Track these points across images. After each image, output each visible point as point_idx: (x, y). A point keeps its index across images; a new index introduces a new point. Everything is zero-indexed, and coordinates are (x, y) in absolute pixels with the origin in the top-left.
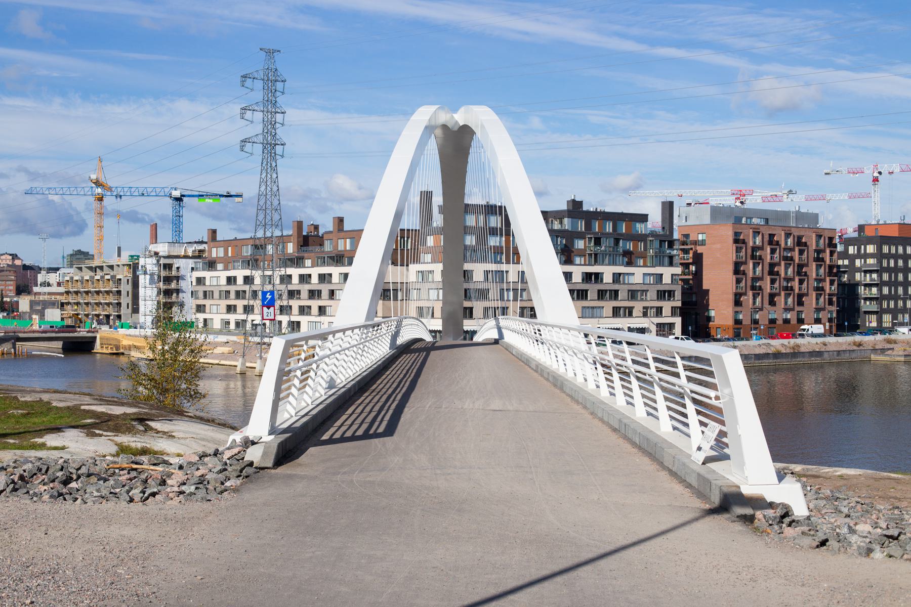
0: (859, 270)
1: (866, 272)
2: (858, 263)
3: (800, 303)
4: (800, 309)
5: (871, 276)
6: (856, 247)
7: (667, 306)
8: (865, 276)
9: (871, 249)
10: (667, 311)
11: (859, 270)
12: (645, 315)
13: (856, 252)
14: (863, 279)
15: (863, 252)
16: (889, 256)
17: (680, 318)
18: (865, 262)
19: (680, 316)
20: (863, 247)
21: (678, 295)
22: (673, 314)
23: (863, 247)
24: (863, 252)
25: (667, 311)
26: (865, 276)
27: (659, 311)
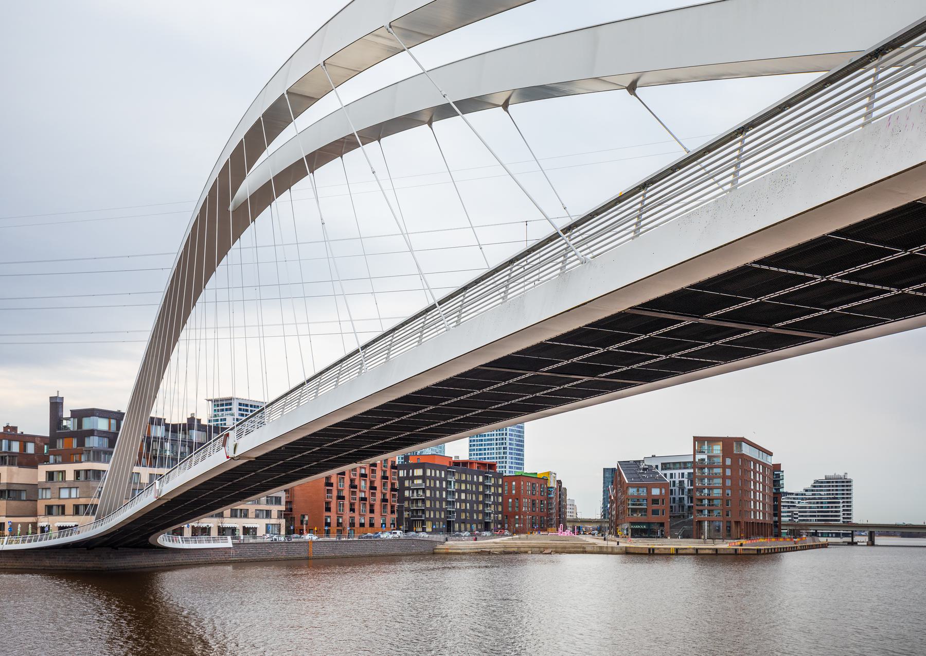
0: (409, 489)
1: (413, 490)
2: (407, 484)
3: (372, 511)
4: (372, 515)
5: (417, 493)
6: (405, 471)
7: (275, 509)
8: (413, 493)
9: (418, 472)
10: (274, 514)
11: (409, 489)
12: (257, 516)
13: (405, 475)
14: (411, 495)
15: (411, 475)
16: (430, 478)
17: (284, 520)
18: (413, 482)
19: (284, 518)
20: (411, 471)
21: (283, 501)
22: (279, 517)
23: (411, 471)
24: (411, 475)
25: (274, 514)
26: (413, 493)
27: (268, 514)
